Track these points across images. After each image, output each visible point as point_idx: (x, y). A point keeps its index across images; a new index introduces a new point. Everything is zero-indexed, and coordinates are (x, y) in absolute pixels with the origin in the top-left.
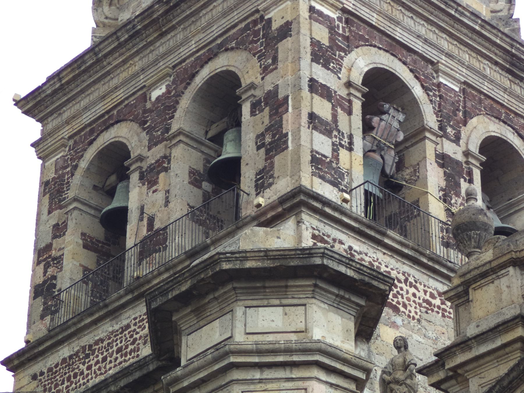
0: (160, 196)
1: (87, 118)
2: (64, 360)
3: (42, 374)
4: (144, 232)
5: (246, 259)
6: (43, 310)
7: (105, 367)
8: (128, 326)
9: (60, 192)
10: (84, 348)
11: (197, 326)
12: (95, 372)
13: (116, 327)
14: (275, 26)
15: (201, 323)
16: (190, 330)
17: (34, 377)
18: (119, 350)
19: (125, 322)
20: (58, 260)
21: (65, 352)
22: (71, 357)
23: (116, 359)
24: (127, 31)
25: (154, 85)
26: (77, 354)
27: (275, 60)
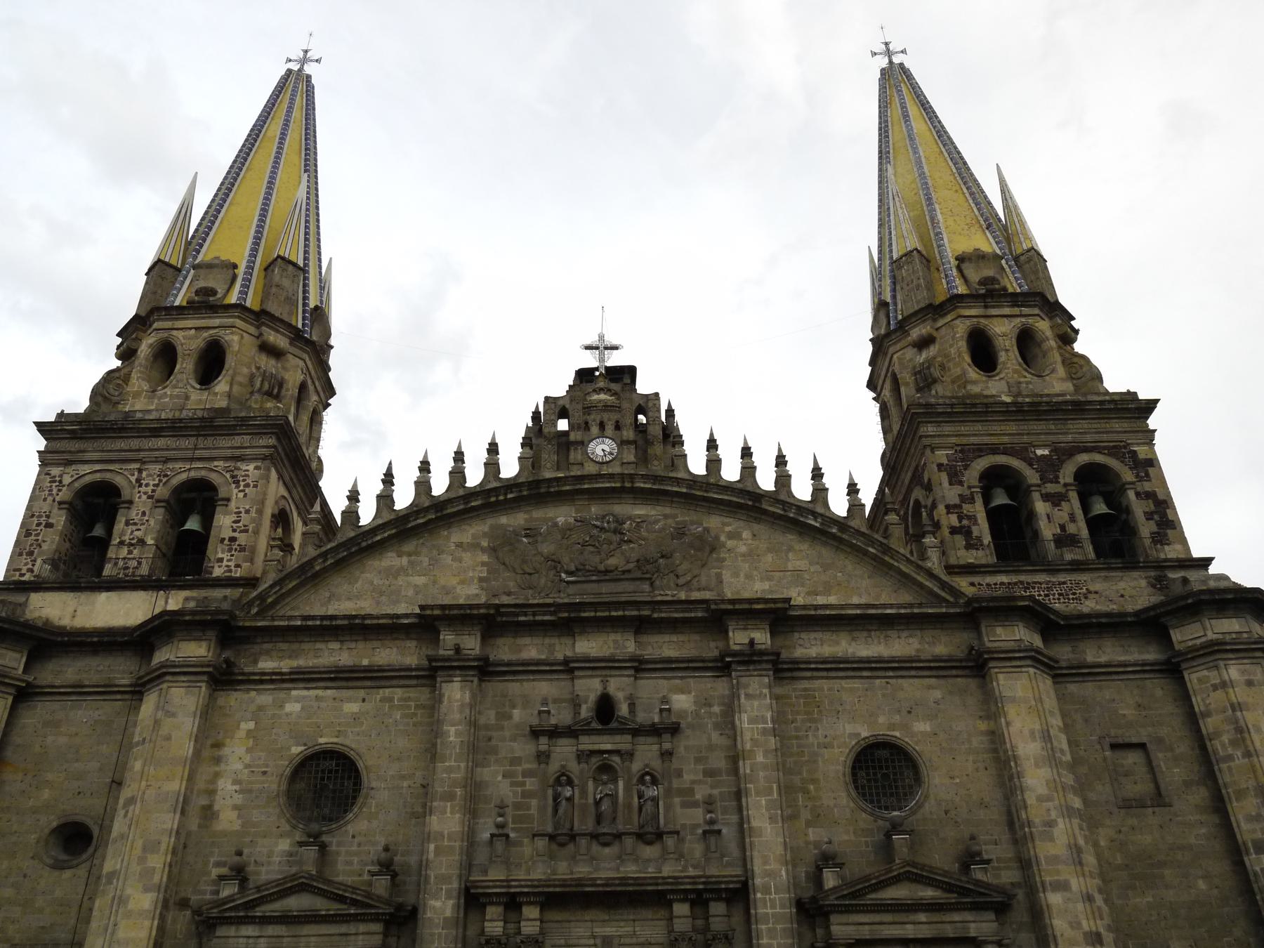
0: (1067, 518)
2: (1002, 583)
8: (1064, 583)
9: (956, 474)
10: (1022, 583)
14: (1142, 456)
20: (973, 519)
21: (1004, 579)
25: (1039, 447)
26: (1016, 584)
27: (1147, 475)
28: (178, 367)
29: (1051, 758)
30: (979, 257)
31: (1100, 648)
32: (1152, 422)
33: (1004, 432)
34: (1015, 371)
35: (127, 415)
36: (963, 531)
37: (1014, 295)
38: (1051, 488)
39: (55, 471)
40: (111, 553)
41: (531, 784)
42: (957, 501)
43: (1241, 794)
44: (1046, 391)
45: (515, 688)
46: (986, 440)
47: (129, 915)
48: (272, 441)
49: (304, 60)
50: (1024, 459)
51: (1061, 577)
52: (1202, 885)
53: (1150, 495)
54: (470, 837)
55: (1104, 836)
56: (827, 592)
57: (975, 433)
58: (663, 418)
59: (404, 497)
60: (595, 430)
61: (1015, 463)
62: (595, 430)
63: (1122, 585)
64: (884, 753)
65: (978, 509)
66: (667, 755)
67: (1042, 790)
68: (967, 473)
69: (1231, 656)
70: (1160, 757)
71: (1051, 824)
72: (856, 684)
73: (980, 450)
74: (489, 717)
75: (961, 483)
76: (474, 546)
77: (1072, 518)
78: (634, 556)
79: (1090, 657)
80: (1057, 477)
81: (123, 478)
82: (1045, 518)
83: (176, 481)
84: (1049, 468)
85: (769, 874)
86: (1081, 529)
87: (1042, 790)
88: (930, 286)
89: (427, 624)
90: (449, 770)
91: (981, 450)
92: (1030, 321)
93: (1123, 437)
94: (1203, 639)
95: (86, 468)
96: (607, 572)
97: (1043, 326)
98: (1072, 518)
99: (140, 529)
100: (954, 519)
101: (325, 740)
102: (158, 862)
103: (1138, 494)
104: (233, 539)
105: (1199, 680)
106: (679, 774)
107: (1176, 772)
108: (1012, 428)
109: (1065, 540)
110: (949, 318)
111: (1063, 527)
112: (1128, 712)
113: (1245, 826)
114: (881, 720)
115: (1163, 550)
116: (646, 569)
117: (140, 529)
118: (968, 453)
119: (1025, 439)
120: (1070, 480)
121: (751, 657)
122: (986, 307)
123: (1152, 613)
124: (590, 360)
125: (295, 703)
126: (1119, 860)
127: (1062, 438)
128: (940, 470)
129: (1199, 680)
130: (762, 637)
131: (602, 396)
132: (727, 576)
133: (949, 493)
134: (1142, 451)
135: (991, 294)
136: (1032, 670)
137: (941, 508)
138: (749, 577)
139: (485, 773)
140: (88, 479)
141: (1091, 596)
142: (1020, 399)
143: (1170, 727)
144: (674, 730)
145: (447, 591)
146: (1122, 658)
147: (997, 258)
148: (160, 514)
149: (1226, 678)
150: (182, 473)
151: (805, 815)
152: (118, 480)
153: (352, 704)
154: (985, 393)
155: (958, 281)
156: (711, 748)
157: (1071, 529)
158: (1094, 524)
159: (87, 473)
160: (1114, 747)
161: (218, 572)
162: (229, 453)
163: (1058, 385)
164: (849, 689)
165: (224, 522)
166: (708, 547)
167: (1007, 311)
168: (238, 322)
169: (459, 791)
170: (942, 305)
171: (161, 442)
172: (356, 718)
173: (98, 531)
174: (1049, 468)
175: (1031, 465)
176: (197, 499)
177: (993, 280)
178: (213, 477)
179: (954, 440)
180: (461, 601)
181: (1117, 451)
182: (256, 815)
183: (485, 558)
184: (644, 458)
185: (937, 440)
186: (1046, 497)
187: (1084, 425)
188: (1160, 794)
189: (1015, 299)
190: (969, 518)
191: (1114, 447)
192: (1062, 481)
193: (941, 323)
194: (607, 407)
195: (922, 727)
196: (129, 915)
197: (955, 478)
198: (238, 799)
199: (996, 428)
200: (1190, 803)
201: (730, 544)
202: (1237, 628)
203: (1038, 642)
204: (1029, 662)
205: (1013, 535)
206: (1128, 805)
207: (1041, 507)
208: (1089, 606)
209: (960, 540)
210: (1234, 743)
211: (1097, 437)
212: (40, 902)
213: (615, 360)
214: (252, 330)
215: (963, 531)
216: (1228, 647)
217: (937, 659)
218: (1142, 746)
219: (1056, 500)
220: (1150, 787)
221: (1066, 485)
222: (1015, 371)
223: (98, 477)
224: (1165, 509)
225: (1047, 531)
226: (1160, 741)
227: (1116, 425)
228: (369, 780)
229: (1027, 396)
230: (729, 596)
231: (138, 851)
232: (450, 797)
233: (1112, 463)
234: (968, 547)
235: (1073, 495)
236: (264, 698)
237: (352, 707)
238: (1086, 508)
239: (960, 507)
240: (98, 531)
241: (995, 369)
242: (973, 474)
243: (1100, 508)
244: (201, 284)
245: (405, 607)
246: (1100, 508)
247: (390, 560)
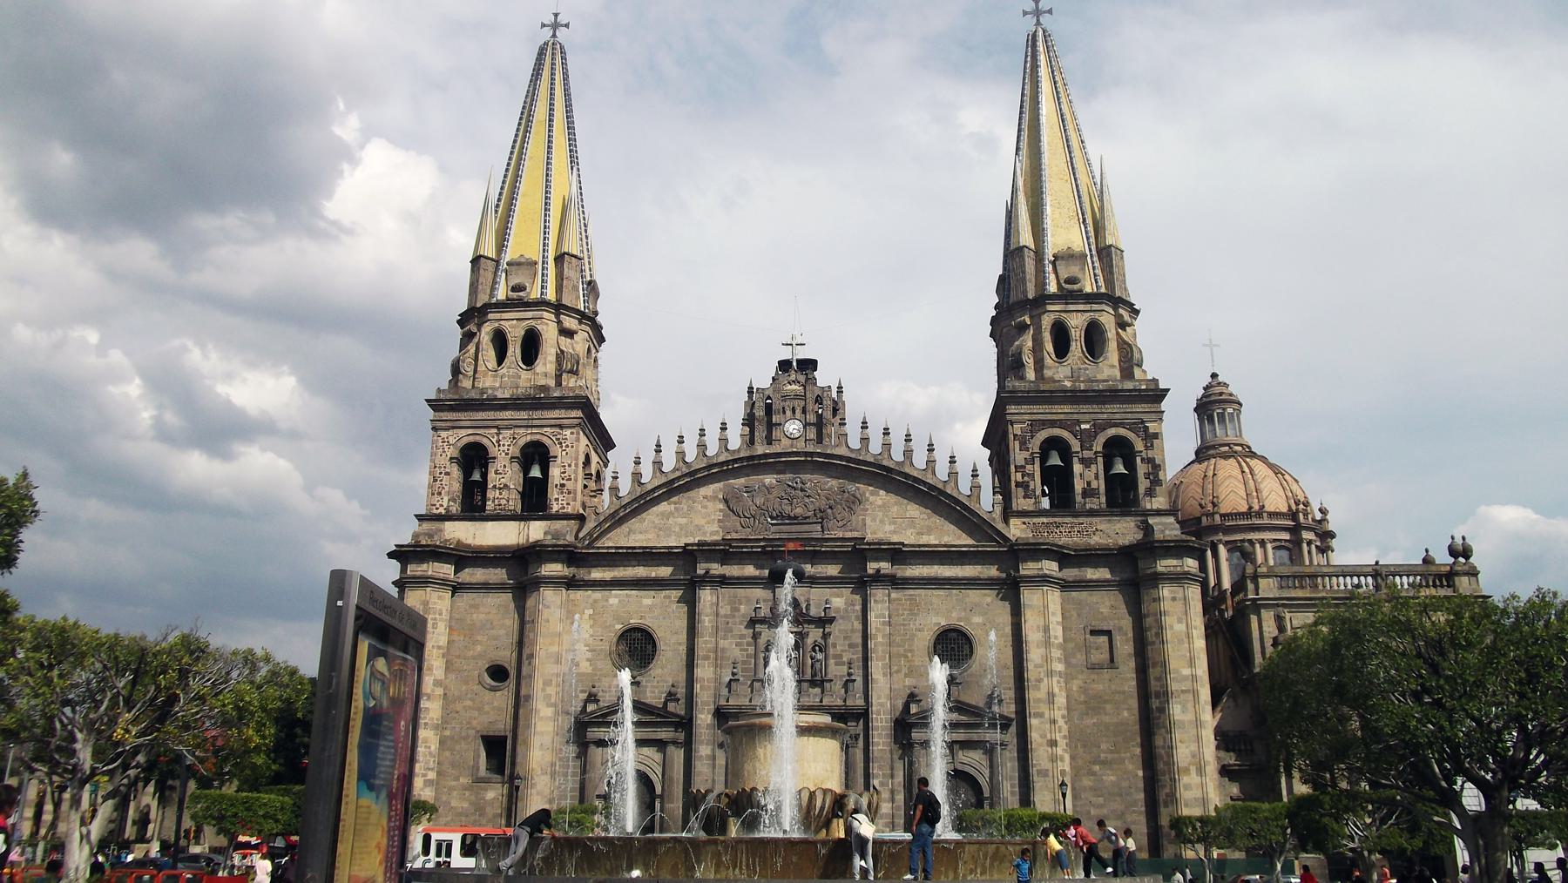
20: (1032, 476)
28: (510, 352)
29: (1047, 643)
32: (1164, 405)
35: (483, 391)
37: (1088, 295)
38: (1087, 454)
39: (444, 434)
40: (490, 494)
41: (751, 650)
43: (1155, 665)
44: (1099, 377)
45: (741, 592)
47: (541, 719)
48: (579, 414)
49: (555, 26)
51: (1081, 520)
52: (1126, 714)
53: (1150, 461)
54: (717, 680)
55: (1075, 685)
56: (929, 531)
57: (1041, 411)
58: (834, 395)
59: (669, 463)
60: (789, 413)
61: (1065, 434)
62: (789, 413)
64: (954, 635)
66: (825, 636)
67: (1039, 661)
70: (1117, 639)
71: (1040, 681)
72: (941, 592)
74: (725, 610)
76: (715, 498)
77: (1097, 477)
78: (811, 507)
81: (488, 438)
83: (522, 442)
84: (1086, 439)
85: (882, 705)
87: (1039, 661)
89: (687, 556)
90: (706, 642)
92: (1096, 315)
95: (463, 432)
96: (796, 518)
97: (1107, 319)
98: (1097, 477)
99: (504, 478)
100: (1019, 477)
101: (634, 621)
102: (551, 690)
104: (563, 485)
106: (834, 646)
107: (1125, 648)
108: (1067, 408)
109: (1089, 492)
112: (1105, 610)
113: (1153, 683)
114: (954, 615)
116: (821, 517)
117: (504, 478)
118: (1036, 425)
120: (1100, 449)
121: (878, 578)
124: (786, 354)
125: (615, 598)
126: (1082, 698)
130: (885, 566)
131: (794, 387)
132: (868, 521)
133: (1018, 456)
134: (1152, 427)
138: (882, 522)
139: (722, 643)
140: (466, 440)
143: (1127, 623)
144: (831, 620)
145: (699, 528)
148: (516, 466)
150: (525, 436)
151: (905, 670)
152: (485, 441)
153: (647, 599)
154: (1057, 377)
155: (1052, 278)
156: (853, 631)
158: (1111, 480)
159: (463, 436)
160: (1093, 633)
161: (555, 508)
162: (553, 422)
163: (1108, 369)
164: (936, 596)
165: (555, 472)
166: (854, 502)
167: (1081, 307)
168: (545, 314)
169: (712, 655)
171: (507, 414)
172: (650, 608)
173: (477, 476)
176: (535, 454)
178: (545, 440)
180: (709, 538)
182: (600, 664)
183: (721, 506)
184: (820, 439)
187: (1116, 407)
188: (1112, 660)
194: (797, 397)
195: (977, 619)
196: (541, 719)
197: (1024, 446)
198: (589, 655)
200: (1128, 668)
201: (872, 498)
206: (1093, 667)
207: (1077, 468)
208: (1096, 540)
210: (1157, 634)
212: (487, 708)
213: (803, 354)
214: (552, 317)
217: (991, 579)
218: (1108, 633)
219: (1086, 463)
220: (1106, 656)
223: (472, 439)
225: (1079, 486)
226: (1120, 629)
228: (661, 645)
230: (869, 537)
231: (540, 685)
232: (706, 658)
233: (1130, 435)
235: (1100, 460)
236: (597, 595)
237: (648, 602)
238: (1108, 466)
240: (477, 476)
242: (1035, 444)
243: (1119, 468)
244: (514, 281)
245: (674, 542)
246: (1119, 468)
247: (664, 507)
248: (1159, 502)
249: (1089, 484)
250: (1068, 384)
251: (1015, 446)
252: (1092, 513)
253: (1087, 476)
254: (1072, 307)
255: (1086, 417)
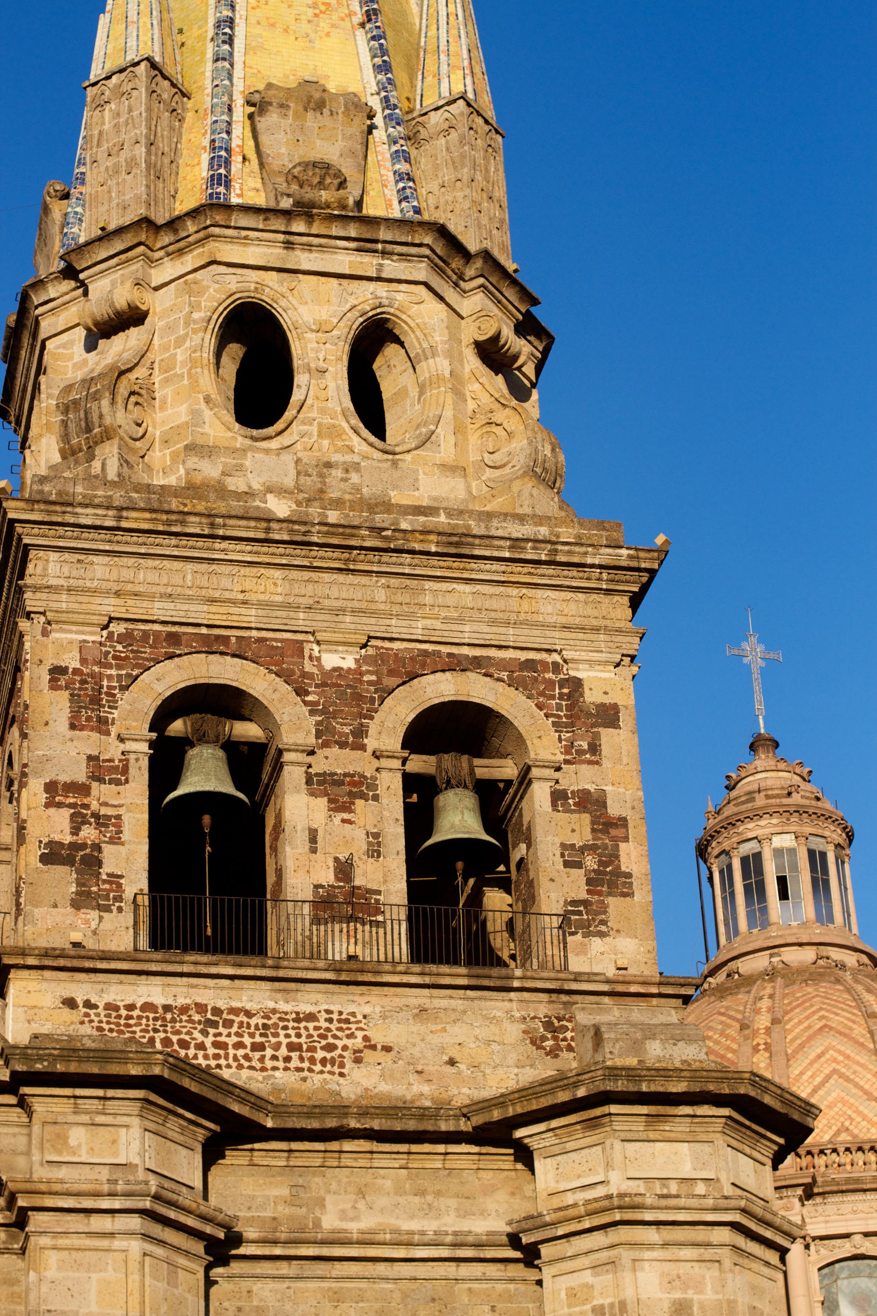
1: (160, 610)
2: (148, 1007)
3: (88, 1004)
4: (327, 877)
5: (765, 1090)
6: (77, 893)
7: (262, 1059)
9: (96, 701)
10: (201, 1008)
11: (643, 1136)
12: (235, 1058)
13: (283, 1006)
14: (592, 696)
15: (652, 1135)
16: (629, 1136)
17: (70, 1003)
18: (291, 1047)
19: (308, 1009)
21: (154, 992)
22: (167, 1008)
23: (288, 1059)
24: (291, 531)
26: (184, 1010)
27: (594, 748)
30: (313, 98)
31: (361, 1193)
33: (256, 593)
34: (329, 432)
36: (78, 859)
42: (80, 774)
44: (396, 497)
46: (199, 613)
50: (286, 676)
53: (591, 803)
57: (170, 588)
63: (458, 1032)
65: (131, 803)
68: (125, 700)
69: (651, 1235)
73: (174, 639)
75: (102, 726)
79: (330, 1222)
80: (360, 732)
82: (302, 838)
86: (388, 878)
88: (160, 169)
91: (173, 642)
92: (401, 296)
93: (556, 639)
94: (600, 1191)
100: (57, 825)
103: (558, 797)
105: (572, 1294)
109: (345, 903)
110: (190, 261)
111: (344, 869)
115: (583, 950)
119: (301, 620)
120: (394, 743)
122: (289, 245)
123: (496, 1115)
127: (397, 627)
128: (54, 685)
129: (572, 1294)
135: (313, 207)
136: (136, 1246)
137: (34, 793)
141: (368, 1055)
142: (314, 512)
146: (413, 1225)
147: (355, 105)
149: (629, 1294)
154: (235, 483)
157: (366, 875)
167: (344, 260)
170: (173, 224)
174: (345, 705)
175: (301, 692)
177: (324, 171)
179: (110, 606)
181: (526, 675)
185: (64, 602)
186: (319, 783)
189: (369, 233)
190: (100, 821)
191: (530, 665)
192: (371, 743)
193: (168, 270)
199: (231, 582)
202: (687, 1171)
203: (187, 1166)
204: (135, 1222)
205: (210, 880)
208: (361, 1083)
209: (65, 879)
211: (489, 633)
215: (78, 859)
216: (648, 1216)
221: (376, 755)
222: (329, 432)
224: (615, 840)
227: (551, 606)
229: (337, 504)
234: (82, 900)
235: (391, 786)
238: (419, 818)
239: (83, 790)
241: (271, 421)
242: (134, 710)
248: (620, 950)
249: (344, 869)
250: (280, 507)
251: (47, 705)
252: (353, 975)
253: (332, 840)
254: (305, 260)
255: (341, 619)
